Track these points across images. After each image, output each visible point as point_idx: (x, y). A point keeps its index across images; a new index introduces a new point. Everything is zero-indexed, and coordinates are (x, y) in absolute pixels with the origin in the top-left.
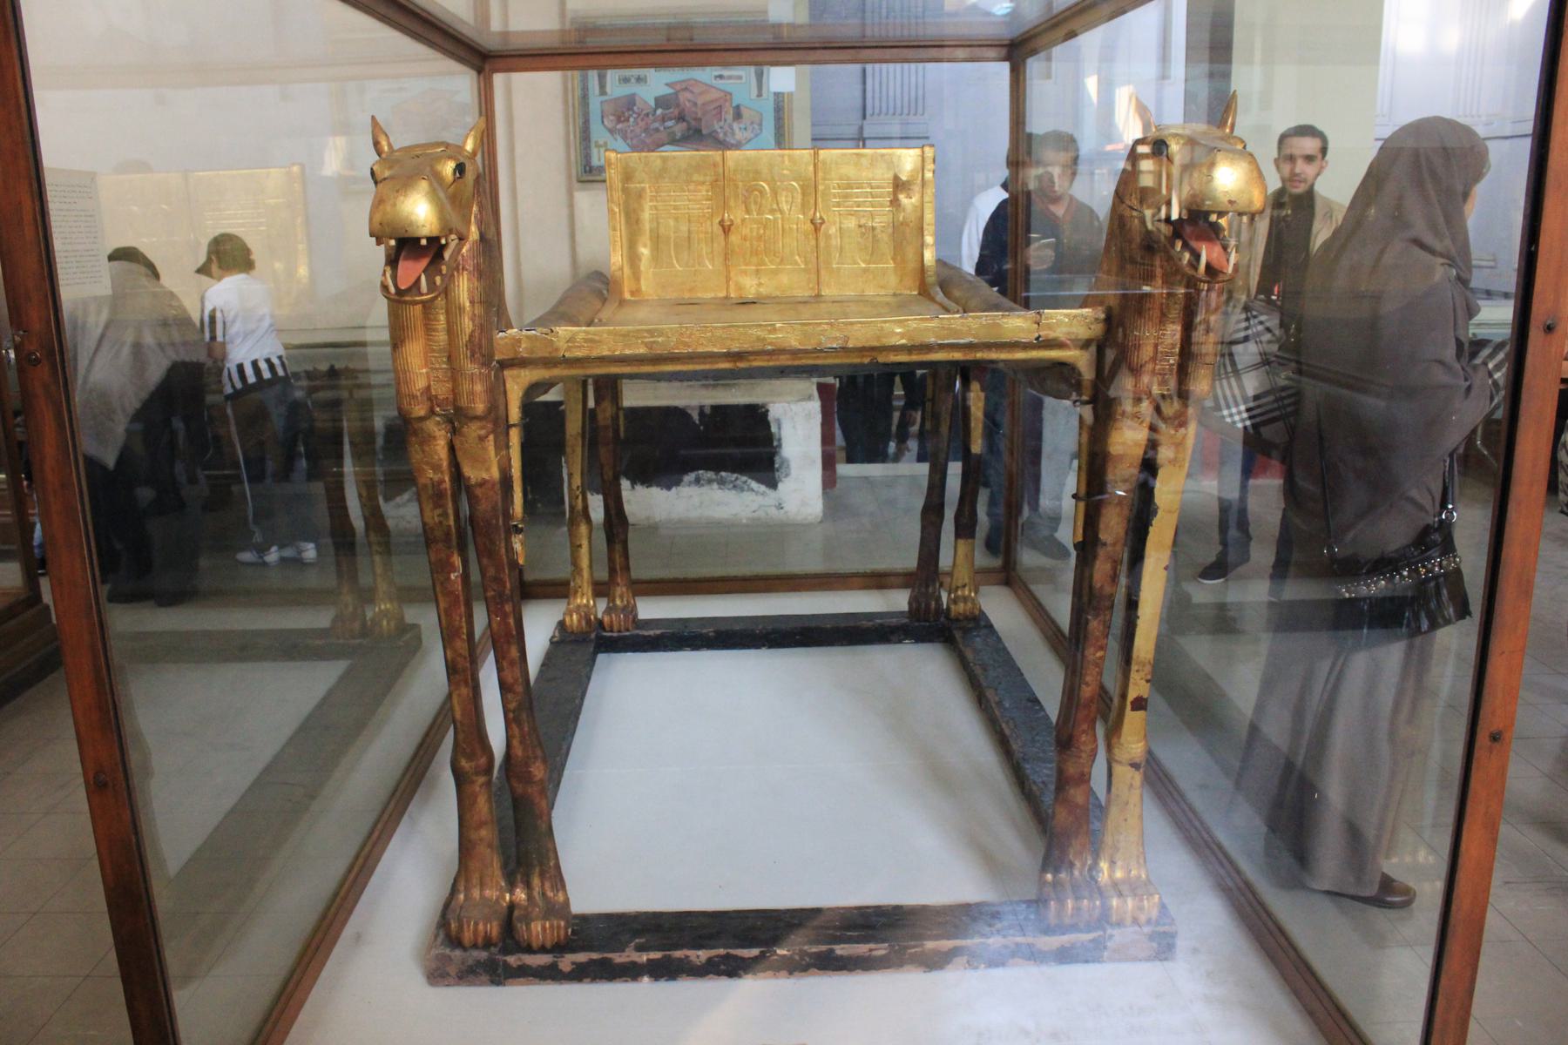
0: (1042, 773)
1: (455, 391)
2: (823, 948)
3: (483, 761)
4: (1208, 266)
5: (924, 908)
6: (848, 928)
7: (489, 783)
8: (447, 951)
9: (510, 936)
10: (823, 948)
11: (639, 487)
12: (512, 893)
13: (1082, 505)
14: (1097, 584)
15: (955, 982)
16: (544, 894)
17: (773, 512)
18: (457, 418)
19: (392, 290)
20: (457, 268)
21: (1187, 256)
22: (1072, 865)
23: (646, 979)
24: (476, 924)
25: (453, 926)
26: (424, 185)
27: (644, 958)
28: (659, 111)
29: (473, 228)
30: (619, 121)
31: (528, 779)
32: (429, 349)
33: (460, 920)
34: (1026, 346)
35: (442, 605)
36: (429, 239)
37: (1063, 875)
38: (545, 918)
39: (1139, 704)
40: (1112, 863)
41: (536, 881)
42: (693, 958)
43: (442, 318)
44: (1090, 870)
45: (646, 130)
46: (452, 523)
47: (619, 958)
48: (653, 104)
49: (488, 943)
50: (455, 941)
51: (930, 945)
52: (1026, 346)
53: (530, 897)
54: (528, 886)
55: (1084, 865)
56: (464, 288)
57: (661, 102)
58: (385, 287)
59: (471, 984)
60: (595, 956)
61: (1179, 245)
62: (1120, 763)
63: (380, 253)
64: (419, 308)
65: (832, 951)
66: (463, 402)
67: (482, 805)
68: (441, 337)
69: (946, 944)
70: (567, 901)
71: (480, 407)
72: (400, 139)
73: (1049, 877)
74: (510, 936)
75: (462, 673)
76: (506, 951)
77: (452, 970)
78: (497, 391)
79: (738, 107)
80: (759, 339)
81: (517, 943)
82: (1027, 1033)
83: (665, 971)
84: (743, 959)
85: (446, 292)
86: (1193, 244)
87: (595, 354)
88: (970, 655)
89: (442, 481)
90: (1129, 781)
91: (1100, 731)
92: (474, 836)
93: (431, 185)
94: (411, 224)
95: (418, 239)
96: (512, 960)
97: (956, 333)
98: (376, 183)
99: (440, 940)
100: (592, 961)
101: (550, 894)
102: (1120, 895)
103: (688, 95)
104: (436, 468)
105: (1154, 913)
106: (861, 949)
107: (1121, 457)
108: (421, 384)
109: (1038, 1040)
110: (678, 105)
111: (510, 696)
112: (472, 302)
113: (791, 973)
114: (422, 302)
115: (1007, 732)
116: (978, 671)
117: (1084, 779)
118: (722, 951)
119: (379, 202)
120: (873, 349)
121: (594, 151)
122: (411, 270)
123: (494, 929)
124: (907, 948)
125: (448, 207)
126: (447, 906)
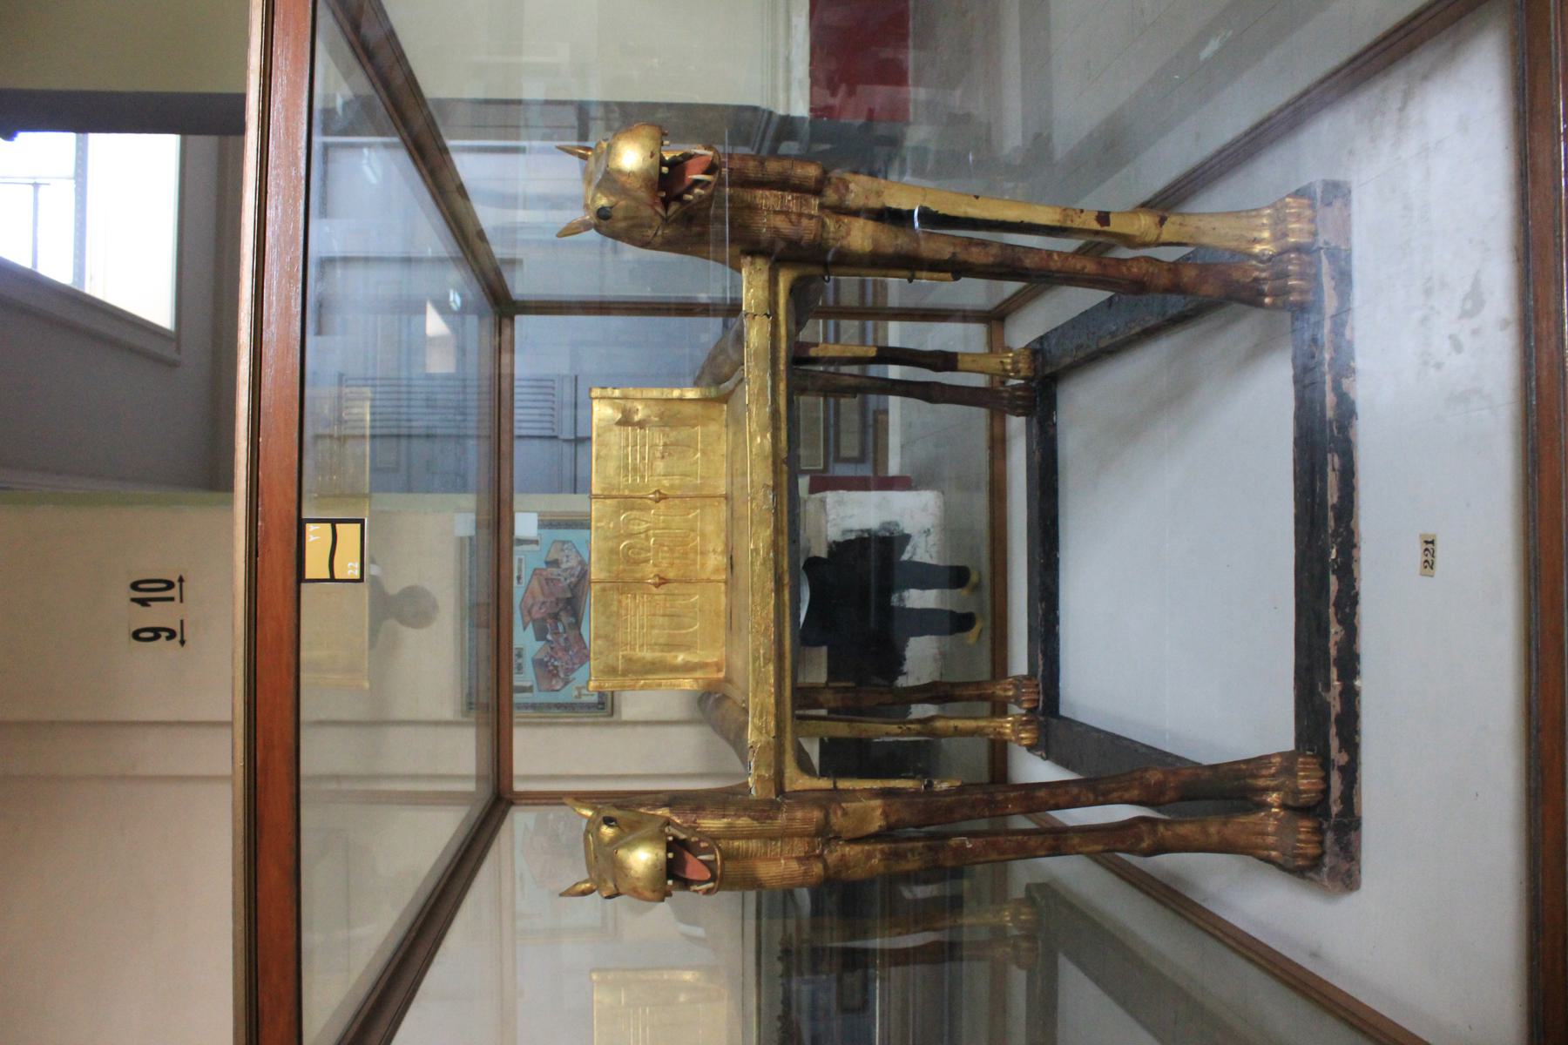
0: (1176, 304)
1: (801, 835)
2: (1331, 514)
3: (1144, 827)
4: (705, 173)
5: (1299, 417)
6: (1314, 491)
7: (1164, 822)
8: (1325, 869)
9: (1312, 809)
10: (1331, 514)
11: (907, 666)
12: (1271, 806)
13: (918, 274)
14: (991, 260)
15: (1363, 392)
16: (1273, 776)
17: (933, 539)
18: (825, 834)
19: (711, 885)
20: (693, 829)
21: (697, 191)
22: (1256, 280)
23: (1357, 683)
24: (1300, 841)
25: (1300, 862)
26: (622, 853)
27: (1336, 684)
28: (549, 637)
29: (659, 812)
30: (556, 676)
31: (1161, 785)
32: (765, 857)
33: (1296, 856)
34: (775, 325)
35: (994, 856)
36: (668, 851)
37: (1266, 288)
38: (1295, 775)
39: (1103, 218)
40: (1256, 241)
41: (1261, 783)
42: (1338, 638)
43: (736, 843)
44: (1262, 262)
45: (566, 650)
46: (920, 844)
47: (1336, 707)
48: (541, 643)
49: (1319, 831)
50: (1316, 863)
51: (1330, 414)
52: (775, 325)
53: (1274, 789)
54: (1266, 790)
55: (1257, 269)
56: (711, 824)
57: (540, 635)
58: (708, 892)
59: (1359, 848)
60: (1333, 730)
61: (690, 197)
62: (1159, 236)
63: (677, 894)
64: (728, 864)
65: (1333, 506)
66: (812, 828)
67: (1183, 830)
68: (753, 845)
69: (1330, 399)
70: (1281, 754)
71: (817, 814)
72: (577, 874)
73: (1267, 300)
74: (1312, 809)
75: (1059, 841)
76: (1326, 814)
77: (1344, 866)
78: (801, 798)
79: (547, 563)
80: (763, 564)
81: (1319, 803)
82: (1424, 320)
83: (1349, 664)
84: (1339, 591)
85: (714, 838)
86: (687, 183)
87: (772, 709)
88: (1067, 360)
89: (882, 852)
90: (1169, 231)
91: (1125, 253)
92: (1215, 838)
93: (622, 846)
94: (655, 866)
95: (668, 861)
96: (1335, 809)
97: (762, 390)
98: (618, 894)
99: (1311, 874)
100: (1339, 734)
101: (1273, 770)
102: (1285, 235)
103: (535, 608)
104: (869, 856)
105: (1306, 201)
106: (1332, 479)
107: (875, 241)
108: (794, 865)
109: (1432, 308)
110: (544, 619)
111: (1083, 799)
112: (724, 816)
113: (1354, 546)
114: (724, 859)
115: (1138, 329)
116: (1081, 354)
117: (1175, 267)
118: (1332, 610)
119: (635, 893)
120: (774, 463)
121: (585, 699)
122: (694, 868)
123: (1305, 825)
124: (1332, 436)
125: (641, 833)
126: (1282, 868)
